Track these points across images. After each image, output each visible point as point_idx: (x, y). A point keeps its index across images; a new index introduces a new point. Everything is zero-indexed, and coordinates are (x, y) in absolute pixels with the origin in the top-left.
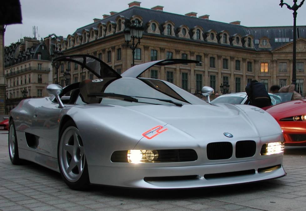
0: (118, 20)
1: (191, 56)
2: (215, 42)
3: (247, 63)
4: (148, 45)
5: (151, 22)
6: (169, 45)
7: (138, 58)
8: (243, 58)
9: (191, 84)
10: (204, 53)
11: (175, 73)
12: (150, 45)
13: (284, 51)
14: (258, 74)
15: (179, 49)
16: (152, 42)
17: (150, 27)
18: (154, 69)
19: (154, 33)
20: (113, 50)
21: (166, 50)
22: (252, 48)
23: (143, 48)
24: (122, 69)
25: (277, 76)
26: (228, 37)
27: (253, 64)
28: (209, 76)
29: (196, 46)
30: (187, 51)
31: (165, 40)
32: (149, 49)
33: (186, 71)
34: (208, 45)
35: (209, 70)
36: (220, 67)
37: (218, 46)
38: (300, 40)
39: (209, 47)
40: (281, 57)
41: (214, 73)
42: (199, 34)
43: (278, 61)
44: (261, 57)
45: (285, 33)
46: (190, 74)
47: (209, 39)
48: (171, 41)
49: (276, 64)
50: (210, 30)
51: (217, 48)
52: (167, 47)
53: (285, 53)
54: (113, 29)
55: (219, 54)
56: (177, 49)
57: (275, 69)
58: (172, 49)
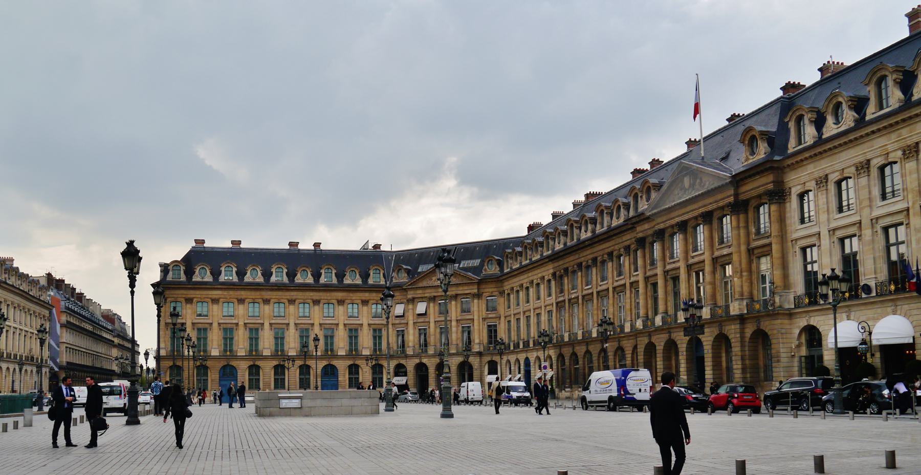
4: (192, 296)
6: (225, 294)
9: (264, 342)
11: (236, 329)
12: (194, 296)
13: (420, 285)
15: (243, 297)
16: (198, 292)
18: (200, 327)
25: (414, 323)
33: (256, 326)
34: (292, 288)
35: (297, 322)
41: (306, 325)
52: (222, 296)
53: (422, 287)
56: (239, 297)
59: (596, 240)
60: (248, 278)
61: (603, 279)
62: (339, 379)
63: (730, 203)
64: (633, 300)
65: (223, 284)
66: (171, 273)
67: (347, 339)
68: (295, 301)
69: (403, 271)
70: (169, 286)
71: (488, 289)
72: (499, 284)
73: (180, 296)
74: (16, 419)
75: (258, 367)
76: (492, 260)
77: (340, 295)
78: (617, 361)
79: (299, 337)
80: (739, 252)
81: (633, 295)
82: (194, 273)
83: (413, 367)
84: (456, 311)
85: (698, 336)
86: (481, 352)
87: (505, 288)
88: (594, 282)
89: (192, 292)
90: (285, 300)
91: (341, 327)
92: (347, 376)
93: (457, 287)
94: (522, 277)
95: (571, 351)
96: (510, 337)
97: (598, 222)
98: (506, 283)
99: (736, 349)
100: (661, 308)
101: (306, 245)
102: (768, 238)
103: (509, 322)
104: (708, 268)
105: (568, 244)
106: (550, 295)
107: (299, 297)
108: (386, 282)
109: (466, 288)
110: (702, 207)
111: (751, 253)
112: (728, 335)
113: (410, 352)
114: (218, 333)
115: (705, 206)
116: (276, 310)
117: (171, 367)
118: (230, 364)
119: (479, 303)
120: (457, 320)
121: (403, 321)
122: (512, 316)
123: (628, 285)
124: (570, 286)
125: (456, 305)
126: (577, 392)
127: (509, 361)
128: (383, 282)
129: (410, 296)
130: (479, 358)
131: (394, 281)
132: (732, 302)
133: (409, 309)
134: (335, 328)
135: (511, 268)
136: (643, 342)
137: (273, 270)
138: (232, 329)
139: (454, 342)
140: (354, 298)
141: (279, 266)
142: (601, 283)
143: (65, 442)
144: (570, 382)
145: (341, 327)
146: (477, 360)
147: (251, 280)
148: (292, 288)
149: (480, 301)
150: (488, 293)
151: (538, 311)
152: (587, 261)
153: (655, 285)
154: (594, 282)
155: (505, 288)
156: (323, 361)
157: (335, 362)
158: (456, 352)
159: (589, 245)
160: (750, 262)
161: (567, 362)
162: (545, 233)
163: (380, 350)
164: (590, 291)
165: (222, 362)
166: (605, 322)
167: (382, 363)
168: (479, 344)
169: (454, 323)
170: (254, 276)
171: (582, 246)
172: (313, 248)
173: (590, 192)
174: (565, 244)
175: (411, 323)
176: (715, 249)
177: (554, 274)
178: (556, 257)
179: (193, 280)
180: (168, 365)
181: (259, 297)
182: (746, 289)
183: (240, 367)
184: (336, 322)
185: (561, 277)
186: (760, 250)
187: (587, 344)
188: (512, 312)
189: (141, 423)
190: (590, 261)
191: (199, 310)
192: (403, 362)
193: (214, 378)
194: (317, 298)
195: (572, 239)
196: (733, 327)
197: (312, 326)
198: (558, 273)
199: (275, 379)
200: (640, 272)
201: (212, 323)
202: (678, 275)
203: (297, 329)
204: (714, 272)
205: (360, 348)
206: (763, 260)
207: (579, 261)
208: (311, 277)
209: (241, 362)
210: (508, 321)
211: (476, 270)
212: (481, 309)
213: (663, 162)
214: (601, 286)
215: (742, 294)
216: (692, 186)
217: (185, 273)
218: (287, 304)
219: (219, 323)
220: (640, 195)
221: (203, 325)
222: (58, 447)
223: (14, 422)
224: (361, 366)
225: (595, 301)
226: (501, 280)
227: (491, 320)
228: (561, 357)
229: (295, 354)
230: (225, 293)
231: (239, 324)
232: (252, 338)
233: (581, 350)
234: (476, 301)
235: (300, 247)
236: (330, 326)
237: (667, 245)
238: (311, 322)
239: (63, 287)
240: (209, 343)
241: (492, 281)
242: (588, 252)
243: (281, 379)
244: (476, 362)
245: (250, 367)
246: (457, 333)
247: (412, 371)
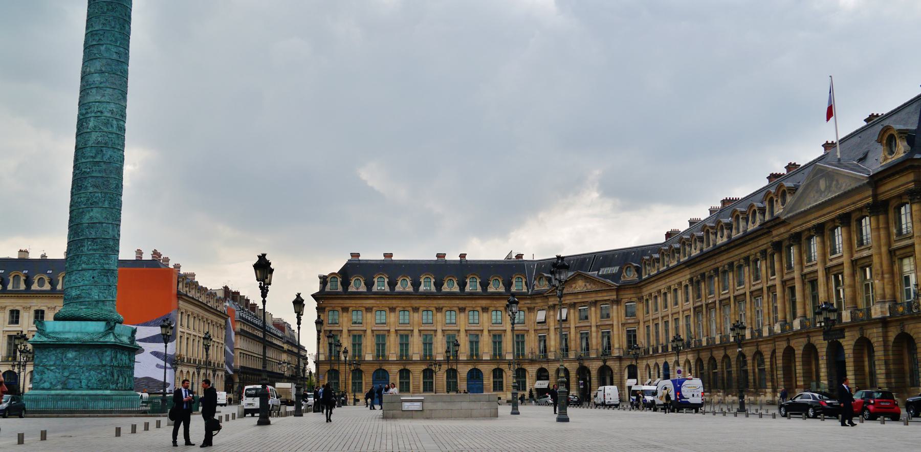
2: (455, 290)
4: (348, 305)
6: (378, 303)
9: (413, 347)
15: (394, 306)
16: (353, 302)
23: (341, 310)
25: (555, 329)
33: (406, 333)
34: (439, 297)
41: (453, 332)
44: (537, 303)
49: (554, 311)
52: (375, 305)
55: (461, 306)
56: (391, 306)
58: (383, 307)
59: (732, 245)
60: (399, 288)
61: (740, 283)
62: (484, 382)
63: (868, 204)
64: (771, 304)
65: (376, 293)
66: (329, 284)
67: (491, 344)
68: (442, 309)
69: (544, 279)
70: (328, 296)
71: (627, 295)
73: (337, 305)
74: (158, 419)
75: (408, 371)
76: (630, 267)
77: (484, 303)
78: (756, 365)
79: (446, 343)
80: (880, 254)
81: (770, 299)
82: (350, 283)
83: (555, 371)
84: (596, 317)
85: (839, 340)
86: (621, 357)
87: (643, 294)
88: (731, 287)
89: (348, 301)
90: (433, 308)
91: (486, 333)
92: (492, 380)
93: (597, 293)
94: (660, 283)
95: (710, 356)
96: (649, 342)
97: (734, 227)
98: (644, 289)
99: (879, 353)
100: (799, 312)
101: (453, 256)
102: (911, 239)
103: (648, 327)
104: (847, 271)
105: (705, 249)
106: (687, 300)
107: (446, 305)
108: (528, 290)
109: (605, 294)
110: (839, 209)
111: (893, 254)
112: (870, 339)
113: (551, 356)
114: (372, 339)
115: (842, 208)
116: (425, 317)
117: (329, 371)
118: (383, 368)
119: (618, 309)
120: (597, 326)
121: (544, 327)
122: (651, 321)
123: (765, 289)
124: (707, 291)
125: (596, 311)
126: (716, 396)
127: (648, 366)
128: (525, 290)
129: (551, 303)
130: (619, 362)
131: (536, 288)
132: (873, 305)
133: (550, 315)
134: (480, 334)
135: (649, 274)
136: (782, 346)
137: (422, 280)
138: (385, 335)
139: (594, 347)
140: (498, 305)
141: (427, 276)
142: (738, 288)
143: (185, 441)
144: (709, 386)
145: (486, 333)
147: (401, 290)
148: (439, 297)
149: (619, 307)
150: (626, 299)
151: (676, 316)
152: (724, 266)
153: (792, 289)
154: (731, 287)
155: (643, 294)
156: (469, 366)
157: (480, 367)
158: (596, 356)
159: (725, 250)
160: (892, 264)
161: (706, 367)
162: (681, 239)
163: (523, 355)
164: (727, 296)
165: (375, 366)
166: (737, 327)
167: (502, 368)
168: (619, 348)
169: (594, 329)
170: (404, 285)
171: (717, 251)
172: (459, 259)
173: (726, 198)
174: (701, 250)
175: (552, 328)
176: (854, 252)
177: (691, 280)
178: (692, 263)
179: (349, 290)
182: (888, 291)
183: (392, 371)
184: (481, 328)
185: (698, 282)
186: (902, 251)
187: (725, 348)
188: (651, 318)
189: (271, 423)
190: (726, 266)
191: (354, 318)
192: (545, 366)
193: (368, 381)
194: (463, 306)
195: (708, 245)
196: (875, 330)
197: (458, 333)
198: (695, 278)
199: (424, 382)
200: (777, 276)
201: (366, 330)
202: (816, 278)
203: (444, 335)
204: (853, 275)
205: (504, 353)
206: (906, 261)
207: (715, 266)
208: (457, 286)
209: (393, 366)
210: (647, 326)
211: (615, 277)
212: (620, 315)
213: (799, 165)
214: (737, 290)
215: (884, 297)
216: (828, 188)
217: (342, 284)
218: (435, 312)
219: (372, 330)
220: (775, 199)
221: (358, 332)
222: (177, 446)
223: (157, 421)
225: (732, 305)
226: (639, 287)
228: (699, 361)
229: (442, 359)
230: (378, 302)
232: (379, 344)
233: (719, 355)
234: (615, 307)
235: (447, 258)
236: (475, 332)
237: (804, 248)
238: (458, 328)
239: (238, 298)
240: (363, 348)
241: (630, 288)
242: (725, 257)
243: (406, 382)
244: (615, 367)
245: (401, 371)
246: (597, 338)
247: (554, 375)
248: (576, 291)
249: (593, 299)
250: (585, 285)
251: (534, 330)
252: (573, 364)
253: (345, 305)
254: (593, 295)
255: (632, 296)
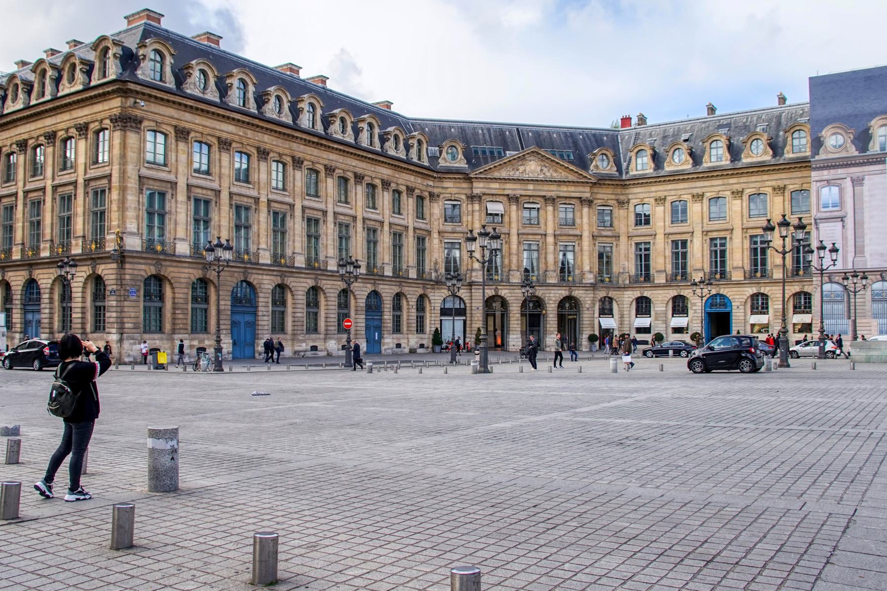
0: (99, 50)
1: (294, 169)
3: (415, 198)
4: (187, 125)
5: (198, 64)
6: (241, 134)
7: (157, 161)
8: (407, 187)
10: (325, 166)
12: (192, 126)
14: (439, 226)
16: (198, 120)
17: (193, 77)
19: (201, 95)
20: (80, 135)
21: (234, 145)
22: (426, 164)
24: (110, 189)
26: (377, 131)
27: (427, 202)
28: (335, 223)
29: (308, 143)
30: (286, 155)
31: (233, 119)
32: (190, 139)
34: (336, 146)
36: (360, 204)
37: (354, 150)
38: (532, 152)
39: (337, 149)
40: (490, 188)
41: (347, 218)
42: (313, 116)
43: (483, 198)
44: (443, 188)
45: (492, 136)
46: (293, 216)
47: (335, 129)
48: (248, 123)
50: (339, 109)
51: (355, 154)
52: (237, 138)
54: (79, 76)
55: (359, 171)
56: (263, 146)
57: (477, 214)
70: (154, 93)
72: (619, 191)
73: (166, 120)
87: (630, 196)
89: (188, 116)
109: (573, 189)
129: (476, 191)
134: (380, 229)
146: (589, 295)
148: (336, 146)
150: (600, 201)
165: (236, 275)
169: (550, 240)
180: (143, 273)
181: (287, 152)
209: (265, 277)
218: (322, 174)
219: (230, 193)
221: (204, 192)
224: (408, 296)
227: (604, 239)
231: (261, 200)
244: (587, 299)
247: (481, 308)
248: (525, 176)
249: (553, 194)
250: (541, 170)
251: (439, 232)
252: (516, 291)
253: (183, 124)
254: (553, 187)
255: (610, 197)
